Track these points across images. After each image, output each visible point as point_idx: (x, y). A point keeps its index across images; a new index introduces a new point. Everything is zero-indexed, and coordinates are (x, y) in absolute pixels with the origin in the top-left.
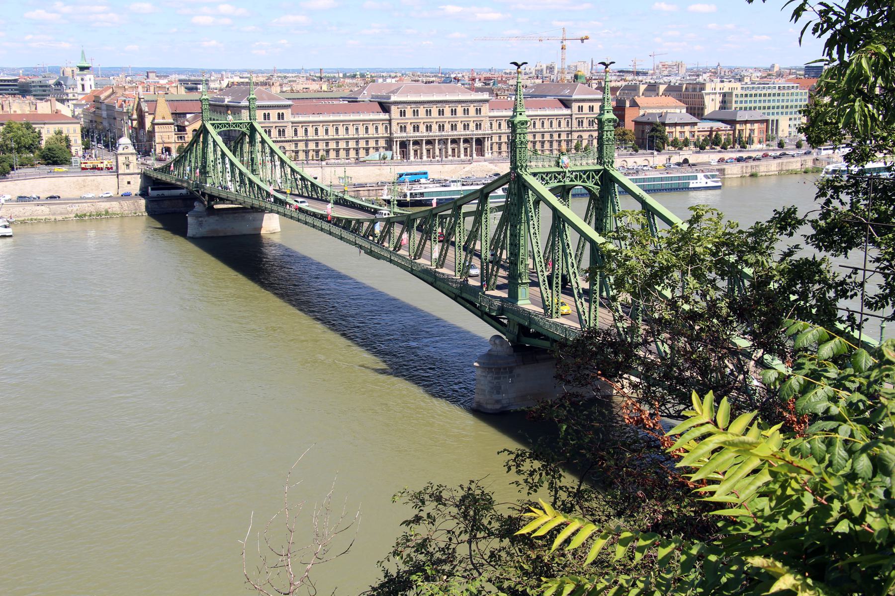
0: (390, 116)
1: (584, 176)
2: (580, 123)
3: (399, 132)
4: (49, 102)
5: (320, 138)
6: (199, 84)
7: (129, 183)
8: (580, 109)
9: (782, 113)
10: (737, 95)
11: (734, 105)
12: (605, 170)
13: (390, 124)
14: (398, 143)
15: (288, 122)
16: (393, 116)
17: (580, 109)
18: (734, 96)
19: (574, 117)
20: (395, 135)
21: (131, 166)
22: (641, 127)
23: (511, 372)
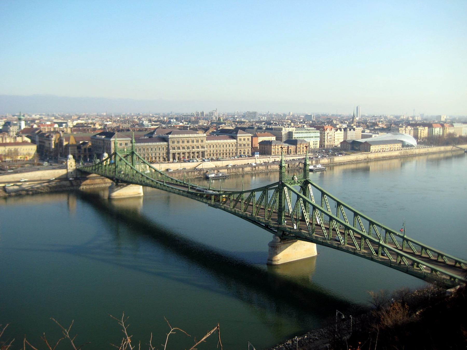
0: (168, 144)
3: (172, 149)
14: (172, 154)
17: (240, 140)
18: (293, 133)
19: (238, 142)
20: (171, 151)
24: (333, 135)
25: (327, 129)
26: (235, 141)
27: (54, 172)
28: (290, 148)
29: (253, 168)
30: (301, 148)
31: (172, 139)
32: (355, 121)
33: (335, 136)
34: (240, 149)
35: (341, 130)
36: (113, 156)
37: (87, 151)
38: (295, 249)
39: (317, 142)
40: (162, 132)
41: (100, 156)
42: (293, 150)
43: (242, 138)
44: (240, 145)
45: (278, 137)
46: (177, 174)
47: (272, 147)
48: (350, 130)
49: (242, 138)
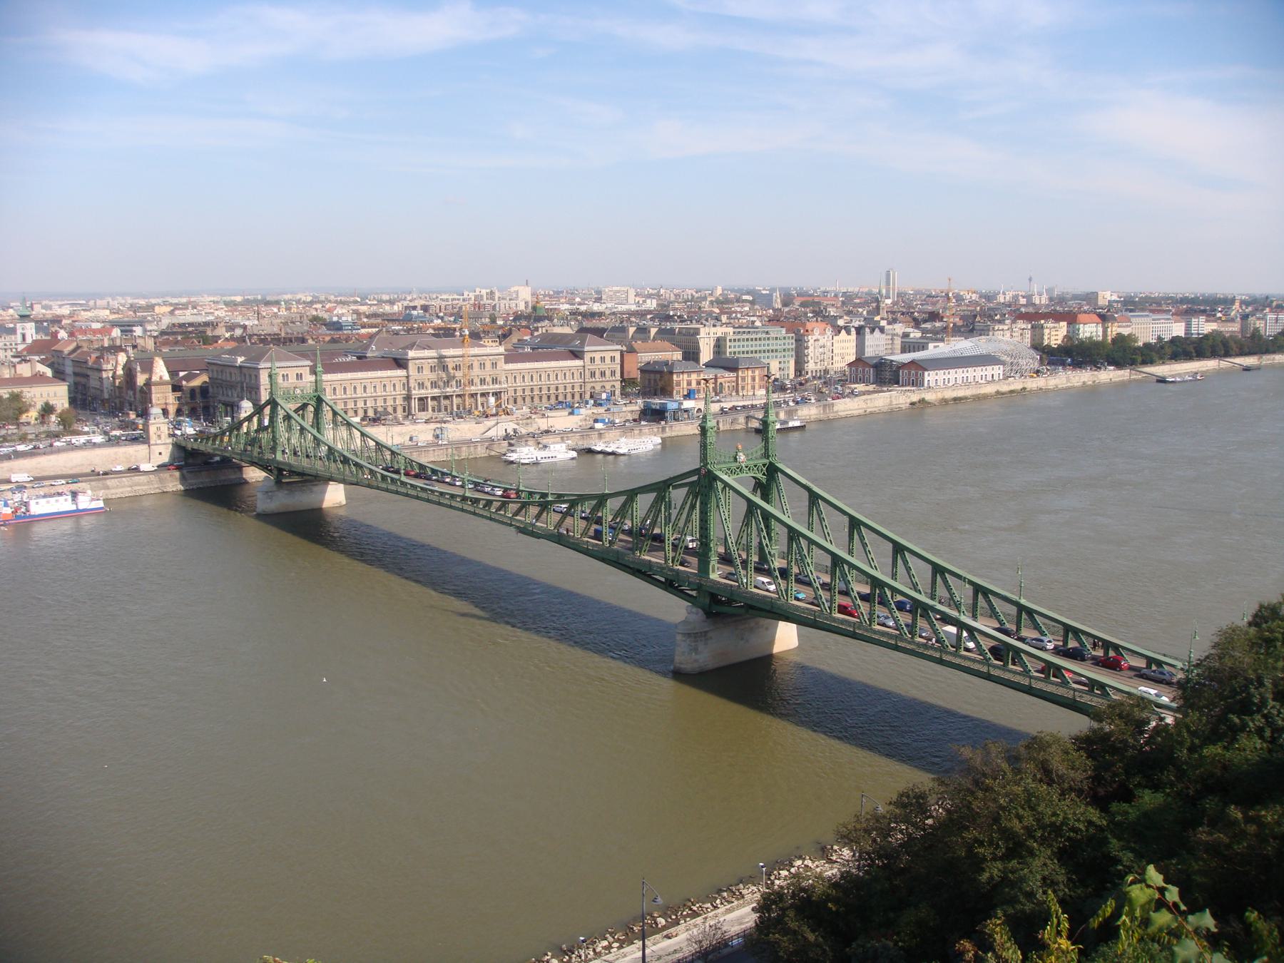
0: (408, 373)
1: (755, 469)
2: (593, 374)
3: (417, 389)
4: (29, 364)
5: (338, 397)
6: (134, 326)
7: (160, 454)
8: (592, 360)
9: (772, 357)
10: (730, 341)
11: (728, 350)
12: (770, 463)
13: (408, 381)
14: (417, 400)
15: (307, 382)
16: (411, 373)
17: (592, 360)
19: (587, 368)
20: (413, 392)
21: (163, 437)
22: (647, 376)
23: (705, 636)
24: (829, 344)
25: (812, 331)
26: (578, 363)
27: (116, 453)
30: (750, 378)
31: (417, 361)
32: (883, 309)
33: (834, 348)
34: (592, 384)
35: (849, 333)
36: (267, 410)
37: (198, 396)
38: (742, 639)
39: (788, 362)
40: (391, 343)
41: (233, 408)
43: (597, 356)
44: (593, 374)
45: (690, 353)
47: (675, 376)
48: (872, 331)
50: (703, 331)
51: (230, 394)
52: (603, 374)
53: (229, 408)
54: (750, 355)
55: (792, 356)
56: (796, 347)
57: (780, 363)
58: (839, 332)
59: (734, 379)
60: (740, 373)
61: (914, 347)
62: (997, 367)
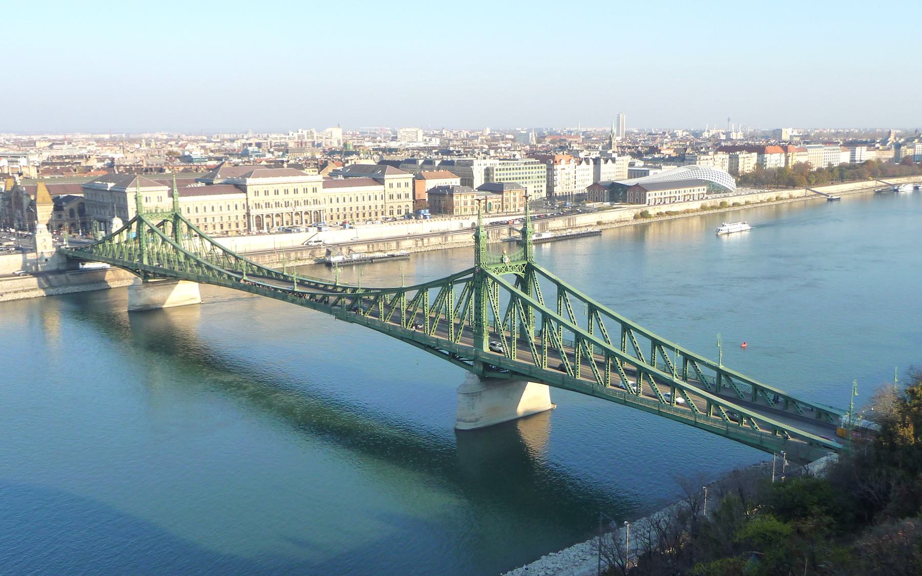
2: (391, 197)
8: (391, 186)
10: (497, 170)
11: (495, 177)
17: (391, 186)
18: (495, 170)
22: (433, 197)
26: (380, 187)
28: (489, 201)
29: (417, 241)
34: (391, 205)
35: (588, 163)
36: (134, 225)
39: (541, 186)
40: (233, 173)
42: (495, 204)
43: (395, 183)
44: (391, 197)
46: (267, 257)
47: (454, 198)
48: (606, 162)
49: (395, 183)
50: (476, 162)
51: (103, 213)
52: (399, 196)
53: (102, 224)
54: (512, 181)
55: (544, 182)
56: (548, 175)
57: (535, 187)
58: (581, 162)
59: (500, 200)
60: (504, 194)
61: (638, 174)
62: (702, 188)
